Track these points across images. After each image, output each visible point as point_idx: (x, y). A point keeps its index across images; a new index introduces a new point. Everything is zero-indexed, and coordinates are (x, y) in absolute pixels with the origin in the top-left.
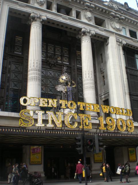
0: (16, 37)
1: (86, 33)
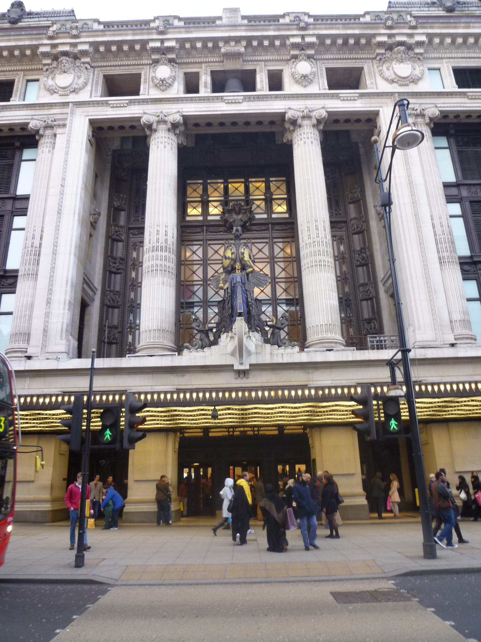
0: (251, 182)
1: (299, 121)
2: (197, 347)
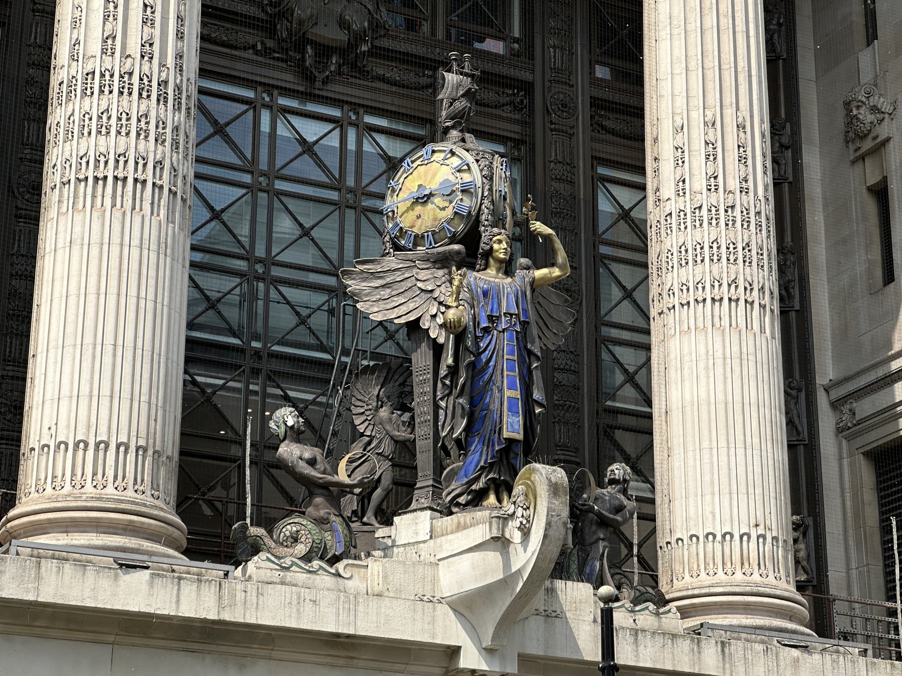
2: (301, 549)
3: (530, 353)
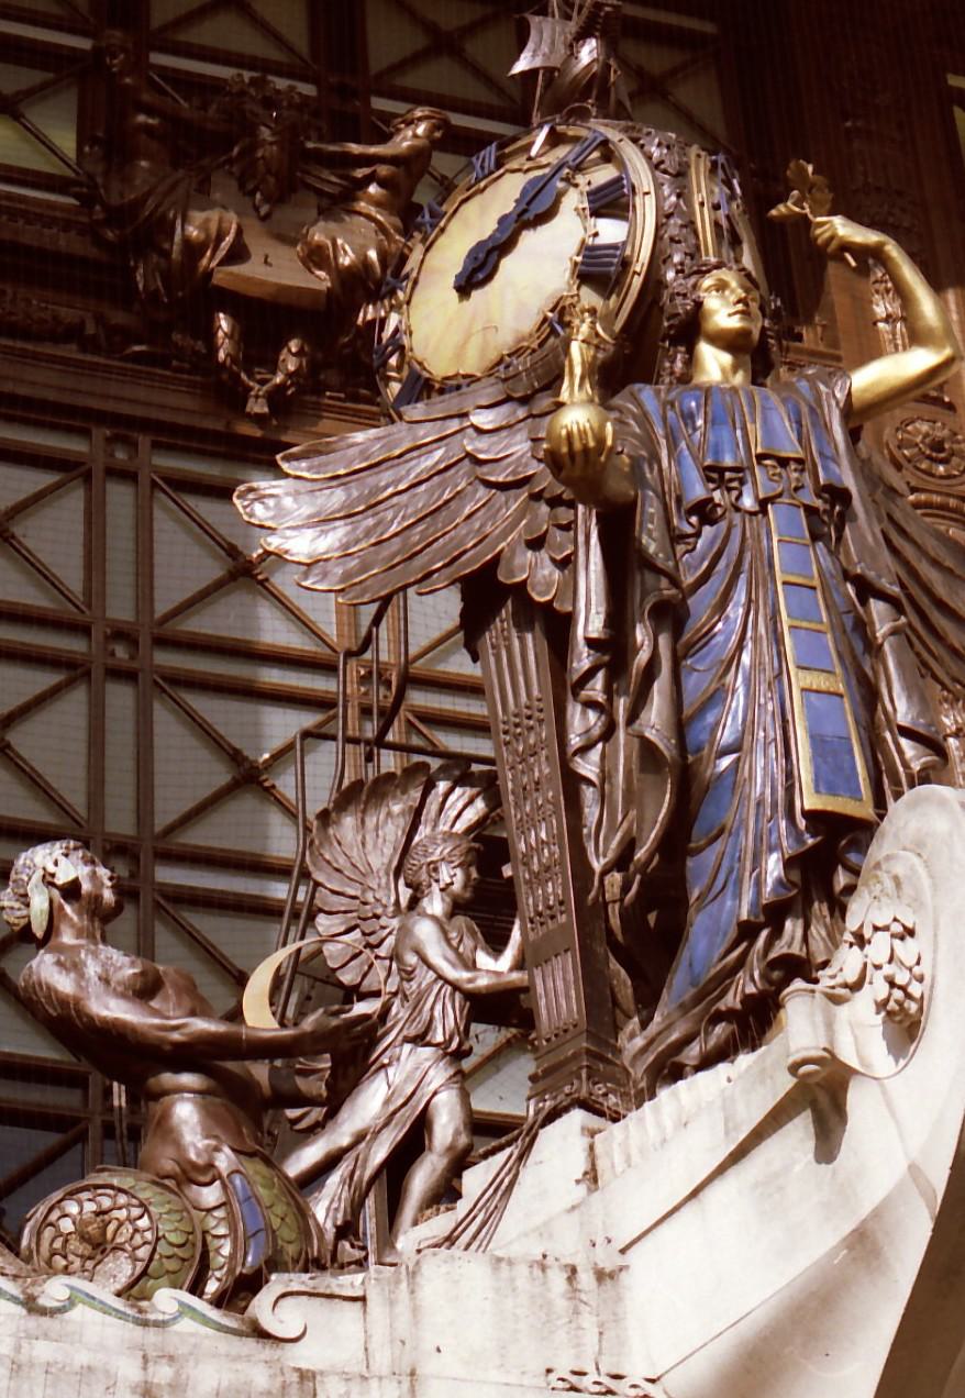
3: (866, 589)
